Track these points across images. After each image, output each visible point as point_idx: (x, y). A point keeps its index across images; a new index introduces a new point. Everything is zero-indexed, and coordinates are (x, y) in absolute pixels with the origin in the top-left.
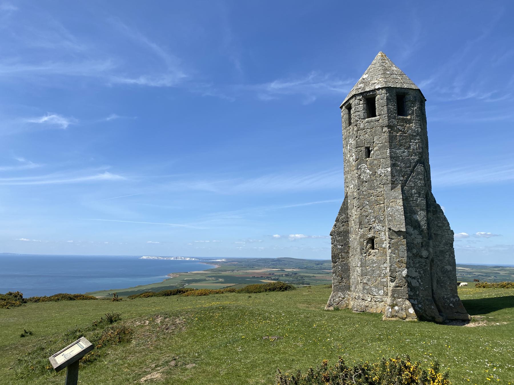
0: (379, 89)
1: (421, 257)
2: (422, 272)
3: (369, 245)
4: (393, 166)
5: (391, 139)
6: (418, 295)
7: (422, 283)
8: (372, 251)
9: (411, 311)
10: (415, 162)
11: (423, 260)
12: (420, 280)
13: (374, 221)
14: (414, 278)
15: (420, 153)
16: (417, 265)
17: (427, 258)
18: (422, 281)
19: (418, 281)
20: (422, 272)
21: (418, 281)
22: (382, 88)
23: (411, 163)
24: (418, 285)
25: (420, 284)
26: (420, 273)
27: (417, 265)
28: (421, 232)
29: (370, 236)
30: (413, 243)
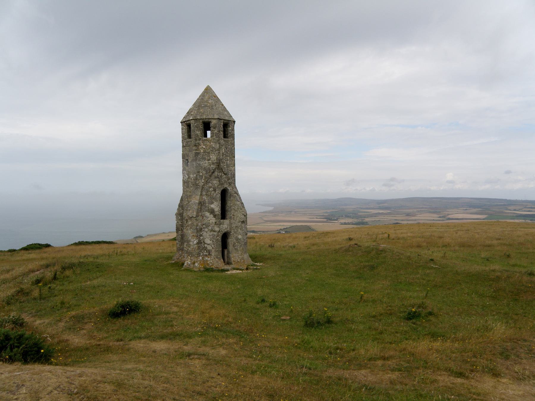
1: (215, 231)
11: (216, 233)
14: (208, 244)
15: (217, 163)
17: (219, 232)
24: (211, 248)
25: (213, 248)
26: (213, 241)
28: (215, 216)
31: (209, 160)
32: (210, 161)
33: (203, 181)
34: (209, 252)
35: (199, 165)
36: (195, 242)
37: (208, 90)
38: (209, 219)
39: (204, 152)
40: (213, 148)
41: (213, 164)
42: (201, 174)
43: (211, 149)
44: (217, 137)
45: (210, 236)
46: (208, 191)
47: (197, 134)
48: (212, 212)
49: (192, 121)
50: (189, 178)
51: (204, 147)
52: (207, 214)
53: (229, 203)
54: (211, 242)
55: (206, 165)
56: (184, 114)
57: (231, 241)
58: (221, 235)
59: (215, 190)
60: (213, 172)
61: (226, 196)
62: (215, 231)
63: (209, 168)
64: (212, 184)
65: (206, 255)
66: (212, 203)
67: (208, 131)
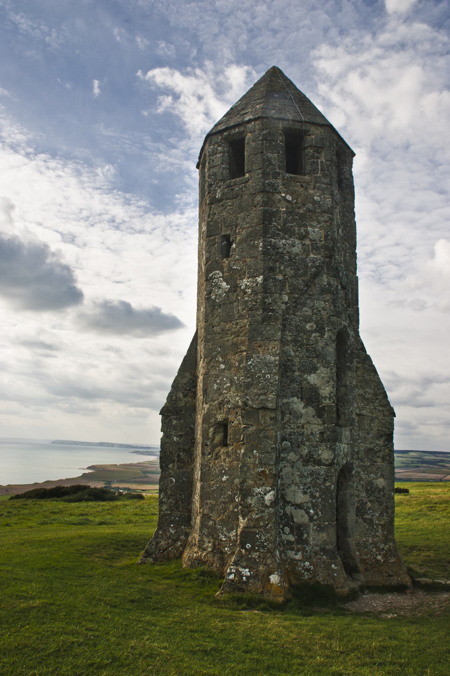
0: (250, 121)
1: (319, 463)
2: (317, 494)
3: (218, 438)
6: (306, 542)
7: (315, 517)
10: (317, 267)
11: (322, 470)
12: (312, 511)
13: (229, 389)
15: (326, 248)
16: (309, 480)
17: (331, 465)
18: (316, 513)
19: (308, 513)
20: (317, 494)
21: (308, 513)
22: (255, 120)
23: (307, 267)
24: (306, 519)
25: (311, 519)
26: (312, 496)
27: (309, 480)
28: (320, 412)
29: (220, 417)
30: (303, 434)
32: (307, 242)
33: (286, 298)
34: (299, 530)
35: (275, 247)
38: (303, 421)
39: (289, 213)
40: (315, 203)
41: (315, 248)
42: (280, 277)
43: (310, 206)
44: (325, 176)
46: (300, 330)
47: (269, 160)
50: (235, 288)
51: (289, 198)
52: (298, 405)
54: (307, 498)
55: (295, 250)
58: (335, 472)
59: (320, 330)
60: (316, 275)
62: (319, 463)
63: (303, 260)
64: (312, 308)
66: (314, 370)
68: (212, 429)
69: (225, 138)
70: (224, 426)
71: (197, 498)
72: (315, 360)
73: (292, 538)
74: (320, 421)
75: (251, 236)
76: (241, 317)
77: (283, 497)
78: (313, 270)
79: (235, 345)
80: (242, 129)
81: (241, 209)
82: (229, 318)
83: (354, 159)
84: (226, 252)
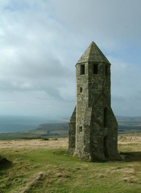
1: (100, 135)
3: (80, 130)
4: (90, 96)
5: (90, 85)
8: (81, 132)
9: (90, 157)
11: (100, 137)
14: (95, 144)
15: (102, 90)
17: (103, 135)
20: (99, 141)
23: (98, 95)
25: (98, 146)
26: (98, 142)
28: (100, 125)
29: (80, 126)
31: (97, 89)
32: (98, 89)
36: (89, 142)
37: (93, 42)
41: (100, 91)
43: (98, 81)
45: (96, 138)
48: (98, 122)
49: (86, 63)
50: (83, 99)
51: (94, 80)
52: (95, 124)
53: (108, 117)
56: (79, 58)
57: (108, 141)
60: (100, 97)
61: (107, 112)
62: (100, 135)
63: (97, 94)
65: (94, 151)
66: (99, 116)
67: (96, 70)
68: (79, 128)
69: (81, 65)
70: (81, 128)
71: (76, 142)
72: (99, 115)
73: (94, 150)
74: (100, 127)
75: (86, 89)
76: (84, 106)
77: (93, 142)
78: (99, 96)
79: (83, 111)
80: (84, 64)
81: (84, 82)
82: (82, 105)
83: (111, 65)
84: (81, 91)
